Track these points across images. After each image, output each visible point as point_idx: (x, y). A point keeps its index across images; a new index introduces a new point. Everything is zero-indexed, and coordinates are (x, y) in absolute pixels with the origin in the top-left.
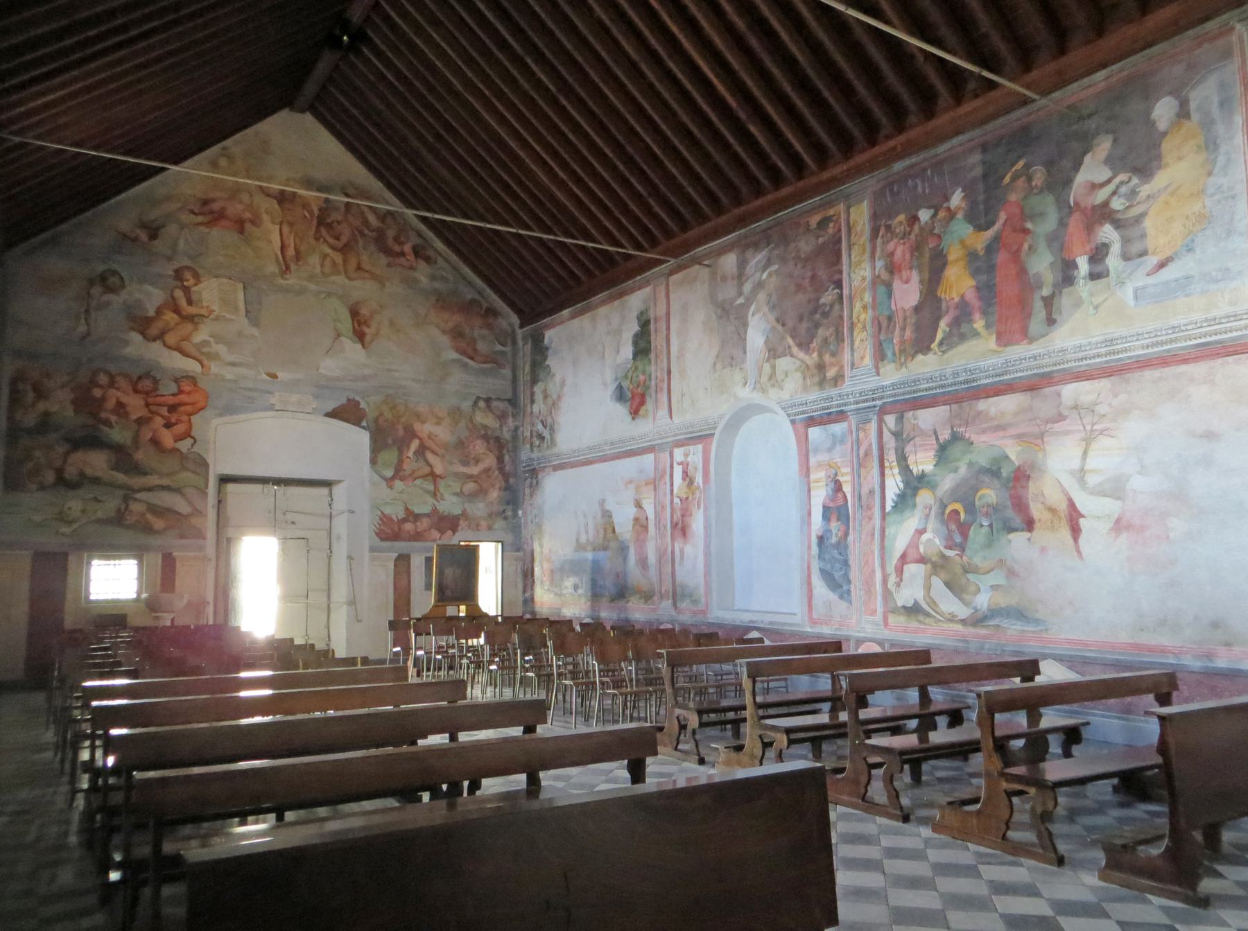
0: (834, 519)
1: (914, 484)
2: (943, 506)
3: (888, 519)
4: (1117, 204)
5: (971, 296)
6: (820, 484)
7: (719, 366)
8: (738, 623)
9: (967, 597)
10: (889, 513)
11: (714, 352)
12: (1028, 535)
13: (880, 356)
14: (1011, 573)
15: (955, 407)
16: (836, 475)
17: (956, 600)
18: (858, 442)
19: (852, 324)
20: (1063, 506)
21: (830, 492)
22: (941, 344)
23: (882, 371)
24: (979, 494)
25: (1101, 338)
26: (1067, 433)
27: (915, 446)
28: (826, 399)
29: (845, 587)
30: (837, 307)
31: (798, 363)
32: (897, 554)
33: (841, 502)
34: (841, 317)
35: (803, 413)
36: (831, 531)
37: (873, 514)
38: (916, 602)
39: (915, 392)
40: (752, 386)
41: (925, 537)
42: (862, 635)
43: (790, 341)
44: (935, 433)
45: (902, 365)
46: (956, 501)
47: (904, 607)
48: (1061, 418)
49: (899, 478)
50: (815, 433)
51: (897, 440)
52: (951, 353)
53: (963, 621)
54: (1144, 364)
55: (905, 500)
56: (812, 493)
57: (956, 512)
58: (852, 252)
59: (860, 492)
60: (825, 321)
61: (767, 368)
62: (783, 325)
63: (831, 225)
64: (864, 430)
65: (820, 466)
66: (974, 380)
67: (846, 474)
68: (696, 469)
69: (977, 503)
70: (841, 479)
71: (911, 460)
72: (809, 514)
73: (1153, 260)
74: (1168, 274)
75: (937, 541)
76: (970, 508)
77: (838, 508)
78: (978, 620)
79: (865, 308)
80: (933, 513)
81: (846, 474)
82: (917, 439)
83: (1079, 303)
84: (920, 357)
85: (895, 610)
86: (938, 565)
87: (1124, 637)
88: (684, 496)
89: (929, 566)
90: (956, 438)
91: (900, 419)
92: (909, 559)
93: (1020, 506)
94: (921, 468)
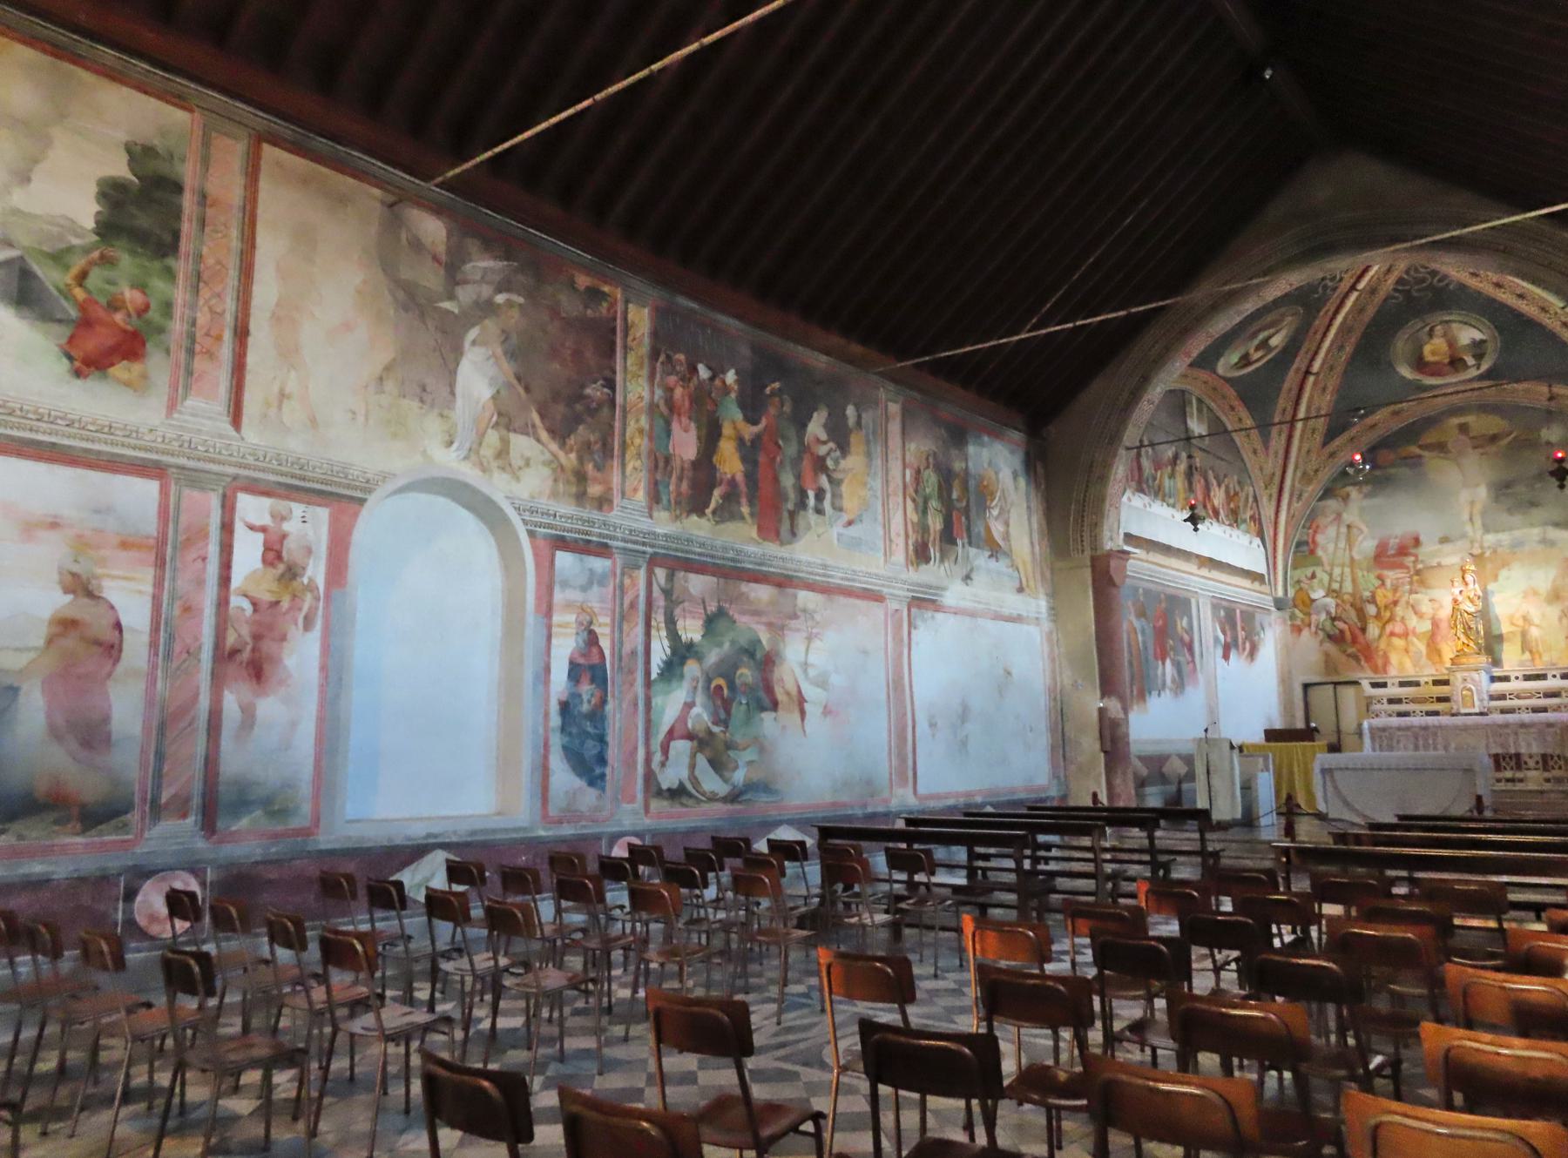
0: (585, 680)
1: (682, 652)
2: (709, 680)
3: (656, 688)
4: (830, 463)
5: (740, 478)
6: (569, 631)
7: (390, 386)
8: (398, 841)
9: (726, 774)
10: (655, 680)
11: (384, 356)
12: (773, 715)
13: (655, 498)
14: (762, 750)
15: (722, 580)
16: (591, 623)
17: (716, 777)
18: (622, 589)
19: (624, 442)
20: (794, 692)
21: (582, 644)
22: (714, 512)
23: (655, 514)
24: (739, 672)
25: (819, 561)
26: (798, 630)
27: (684, 610)
28: (585, 521)
29: (598, 771)
30: (605, 411)
31: (548, 456)
32: (665, 729)
33: (595, 660)
34: (612, 427)
35: (549, 526)
36: (580, 696)
37: (635, 680)
38: (681, 784)
39: (687, 552)
40: (463, 453)
41: (697, 710)
42: (615, 829)
43: (535, 417)
44: (704, 602)
45: (677, 518)
46: (721, 675)
47: (669, 790)
48: (795, 616)
49: (666, 643)
50: (564, 559)
51: (666, 599)
52: (722, 526)
53: (725, 800)
54: (848, 592)
55: (672, 668)
56: (554, 641)
57: (719, 688)
58: (629, 356)
59: (620, 650)
60: (589, 420)
61: (493, 437)
62: (527, 389)
63: (605, 305)
64: (631, 577)
65: (569, 606)
66: (738, 561)
67: (606, 625)
68: (309, 551)
69: (737, 681)
70: (598, 630)
71: (680, 624)
72: (547, 670)
73: (845, 518)
74: (853, 531)
75: (706, 717)
76: (732, 686)
77: (592, 667)
78: (734, 797)
79: (641, 431)
80: (700, 685)
81: (606, 625)
82: (686, 604)
83: (809, 528)
84: (694, 518)
85: (659, 793)
86: (702, 742)
87: (828, 798)
88: (267, 597)
89: (695, 743)
90: (721, 613)
91: (670, 577)
92: (676, 734)
93: (769, 690)
94: (689, 636)
